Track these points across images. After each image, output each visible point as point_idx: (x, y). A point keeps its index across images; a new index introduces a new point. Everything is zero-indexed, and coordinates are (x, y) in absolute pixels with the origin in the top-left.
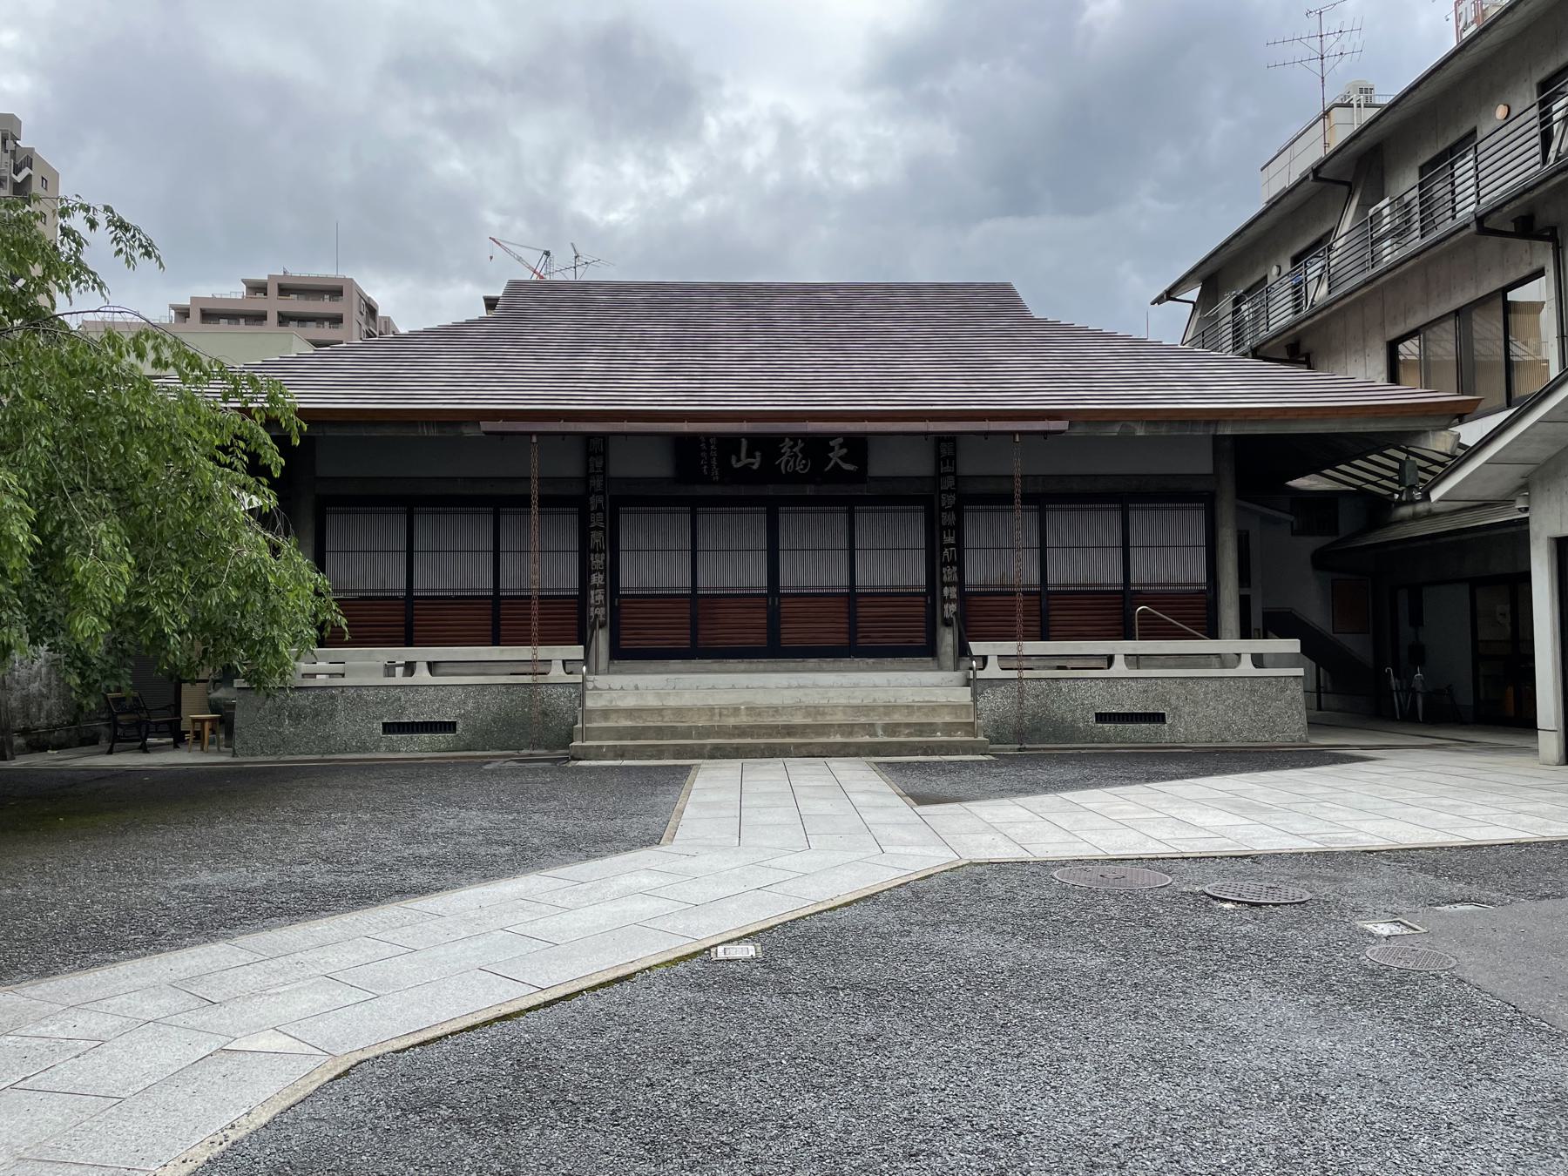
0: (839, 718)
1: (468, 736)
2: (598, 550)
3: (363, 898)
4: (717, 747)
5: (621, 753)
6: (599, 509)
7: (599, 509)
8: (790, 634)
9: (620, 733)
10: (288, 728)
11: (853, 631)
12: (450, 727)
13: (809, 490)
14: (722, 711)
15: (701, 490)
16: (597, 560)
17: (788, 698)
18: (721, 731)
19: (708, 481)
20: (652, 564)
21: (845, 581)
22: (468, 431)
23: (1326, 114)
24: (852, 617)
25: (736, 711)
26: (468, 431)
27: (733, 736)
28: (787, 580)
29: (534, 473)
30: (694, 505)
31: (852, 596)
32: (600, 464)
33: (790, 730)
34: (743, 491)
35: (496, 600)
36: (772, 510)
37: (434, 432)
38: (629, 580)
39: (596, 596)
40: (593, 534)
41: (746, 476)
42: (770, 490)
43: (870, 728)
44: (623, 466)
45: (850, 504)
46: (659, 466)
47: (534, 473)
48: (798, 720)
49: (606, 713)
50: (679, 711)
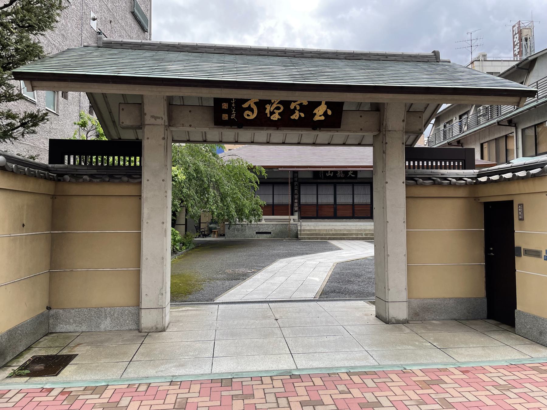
0: (354, 232)
2: (295, 194)
3: (303, 254)
8: (339, 214)
9: (308, 234)
10: (236, 232)
11: (353, 213)
12: (270, 233)
13: (344, 181)
15: (319, 181)
16: (296, 197)
17: (342, 228)
18: (329, 234)
20: (308, 197)
21: (351, 201)
22: (275, 170)
23: (472, 63)
24: (353, 210)
26: (275, 170)
28: (338, 201)
30: (317, 184)
31: (353, 205)
33: (344, 234)
34: (329, 181)
36: (335, 185)
38: (303, 201)
39: (296, 205)
41: (329, 177)
42: (335, 181)
43: (362, 234)
44: (300, 176)
45: (353, 184)
46: (310, 176)
48: (345, 232)
49: (304, 230)
50: (319, 230)
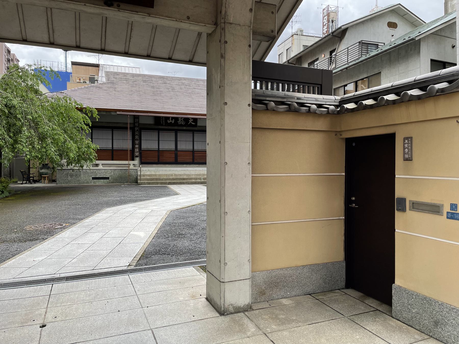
0: (193, 177)
1: (112, 180)
2: (136, 138)
3: (136, 201)
4: (170, 182)
5: (149, 183)
6: (137, 130)
7: (137, 130)
8: (179, 159)
9: (148, 180)
10: (69, 178)
11: (193, 159)
12: (108, 178)
13: (184, 128)
14: (169, 175)
15: (160, 127)
16: (137, 142)
17: (182, 173)
18: (170, 179)
19: (162, 125)
20: (149, 143)
21: (192, 148)
22: (113, 113)
23: (292, 36)
24: (193, 156)
25: (172, 175)
26: (113, 113)
27: (172, 180)
28: (179, 147)
29: (129, 122)
30: (159, 130)
32: (137, 120)
33: (184, 179)
34: (170, 128)
35: (113, 150)
36: (176, 131)
37: (104, 113)
38: (144, 146)
39: (137, 150)
40: (136, 136)
41: (171, 124)
42: (176, 128)
43: (200, 179)
44: (142, 121)
45: (193, 131)
46: (152, 122)
47: (129, 122)
48: (185, 177)
49: (144, 175)
50: (160, 175)
